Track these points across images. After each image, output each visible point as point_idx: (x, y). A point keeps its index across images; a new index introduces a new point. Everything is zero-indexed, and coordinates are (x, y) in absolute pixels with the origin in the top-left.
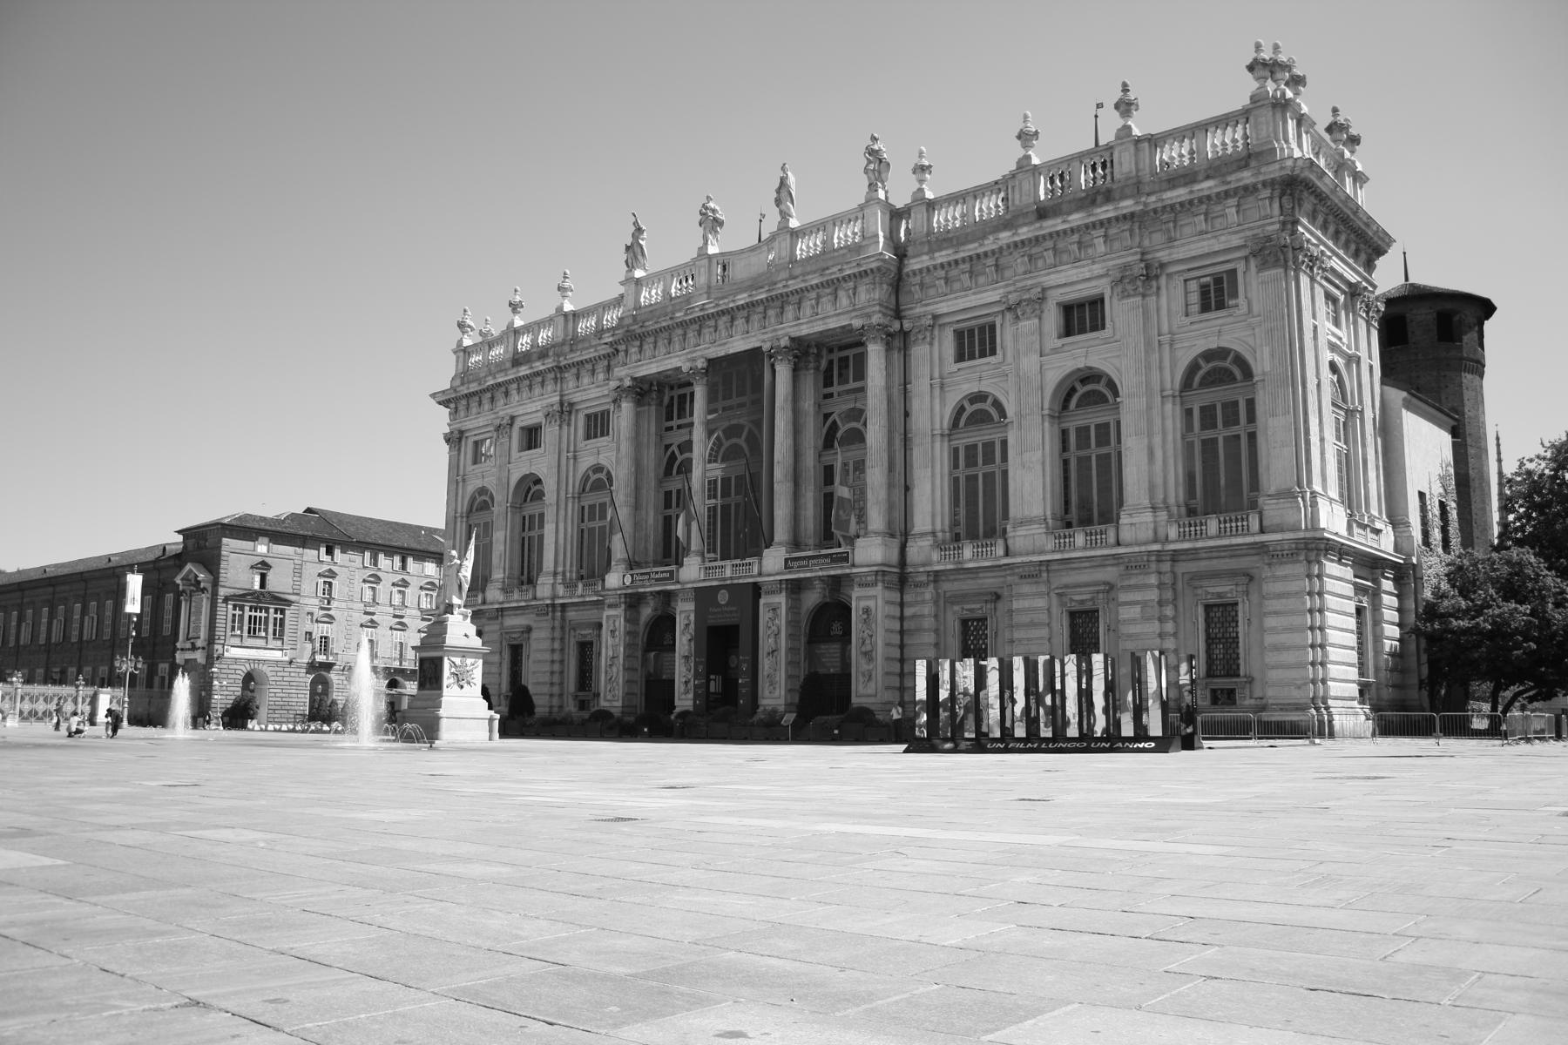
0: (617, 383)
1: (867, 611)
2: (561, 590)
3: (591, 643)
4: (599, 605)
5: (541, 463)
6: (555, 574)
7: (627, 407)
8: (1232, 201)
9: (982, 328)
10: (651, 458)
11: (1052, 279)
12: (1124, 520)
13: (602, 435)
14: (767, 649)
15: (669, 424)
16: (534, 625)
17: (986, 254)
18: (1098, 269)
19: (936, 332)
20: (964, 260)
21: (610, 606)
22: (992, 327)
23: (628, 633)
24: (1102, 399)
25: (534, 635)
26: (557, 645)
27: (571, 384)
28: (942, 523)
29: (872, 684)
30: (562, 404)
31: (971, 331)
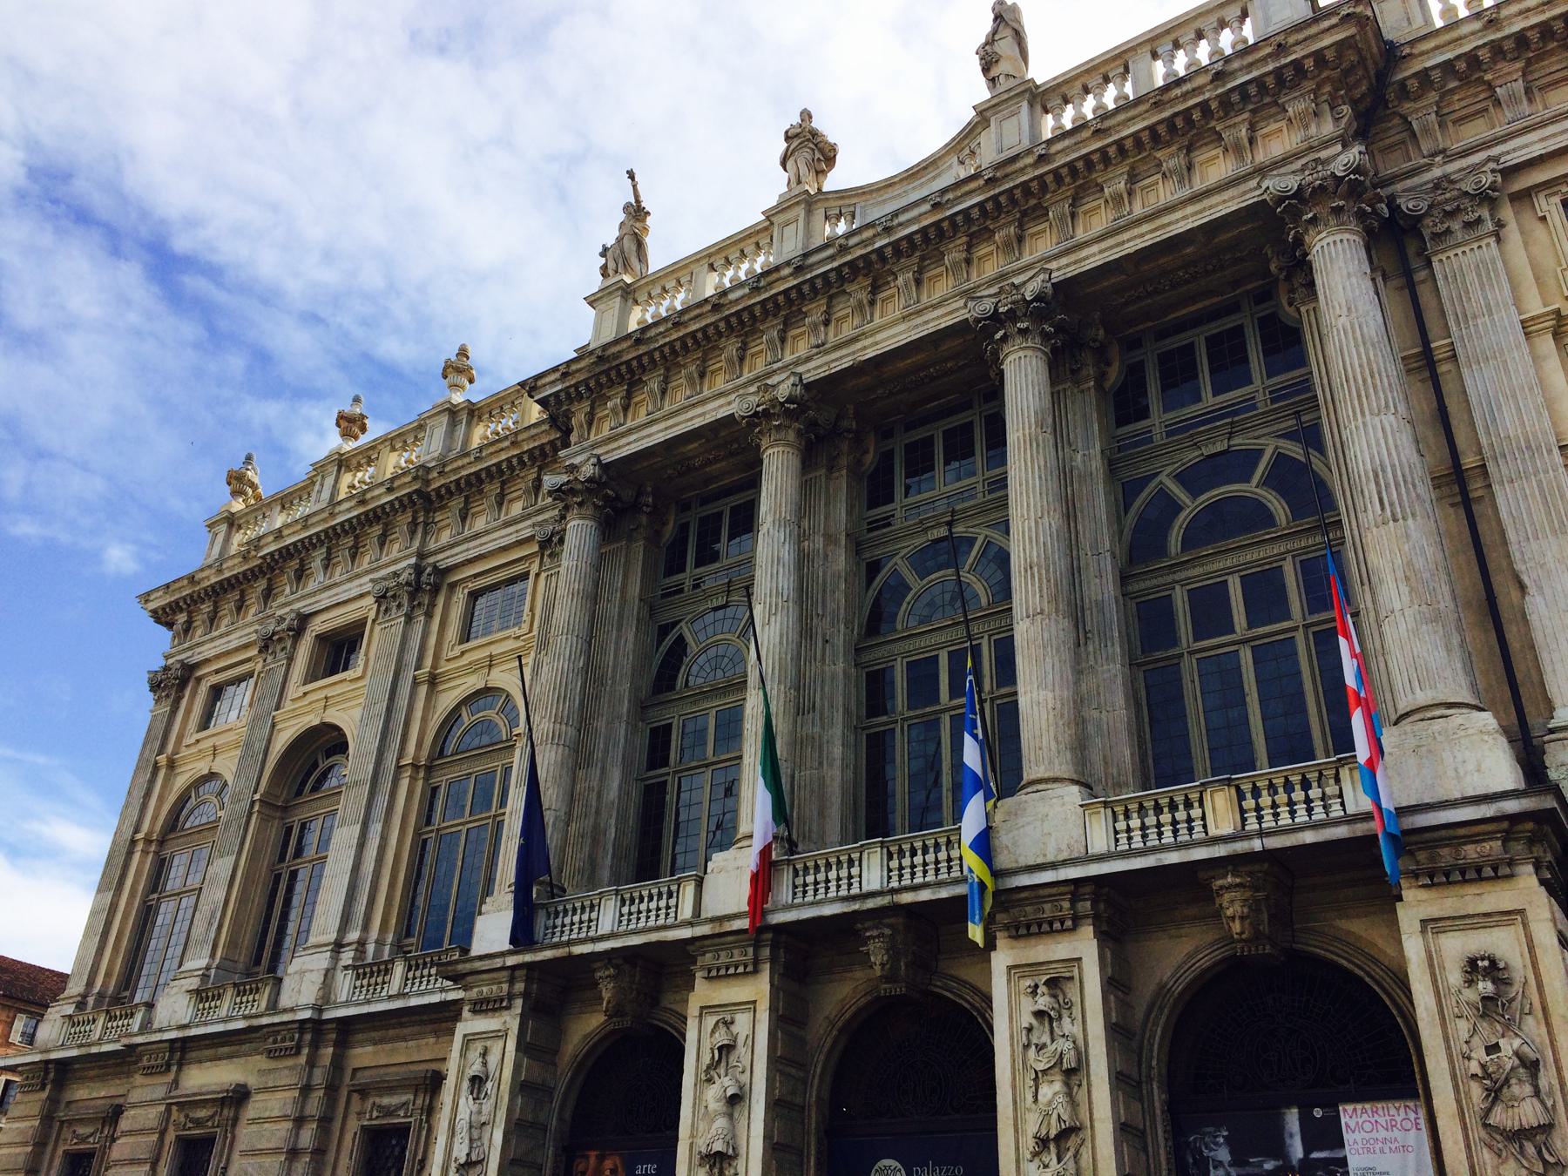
0: (565, 478)
1: (1482, 967)
2: (344, 984)
3: (403, 1131)
4: (442, 1017)
5: (350, 704)
6: (338, 946)
7: (579, 532)
10: (624, 648)
14: (1032, 1125)
16: (252, 1081)
19: (1507, 212)
21: (482, 1007)
23: (521, 1087)
25: (252, 1110)
26: (307, 1137)
27: (445, 537)
30: (418, 569)
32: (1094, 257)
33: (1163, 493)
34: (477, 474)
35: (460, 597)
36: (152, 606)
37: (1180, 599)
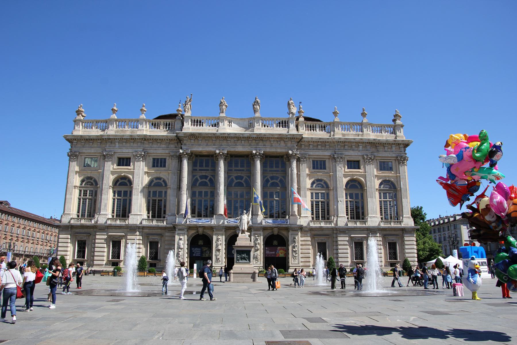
8: (393, 146)
9: (321, 161)
11: (347, 153)
12: (369, 219)
13: (161, 166)
15: (196, 168)
17: (328, 142)
18: (360, 154)
20: (321, 142)
21: (179, 230)
22: (324, 162)
24: (356, 187)
27: (147, 146)
28: (309, 214)
29: (297, 261)
31: (317, 161)
32: (268, 150)
33: (268, 179)
34: (157, 139)
35: (151, 158)
36: (68, 138)
37: (268, 193)
